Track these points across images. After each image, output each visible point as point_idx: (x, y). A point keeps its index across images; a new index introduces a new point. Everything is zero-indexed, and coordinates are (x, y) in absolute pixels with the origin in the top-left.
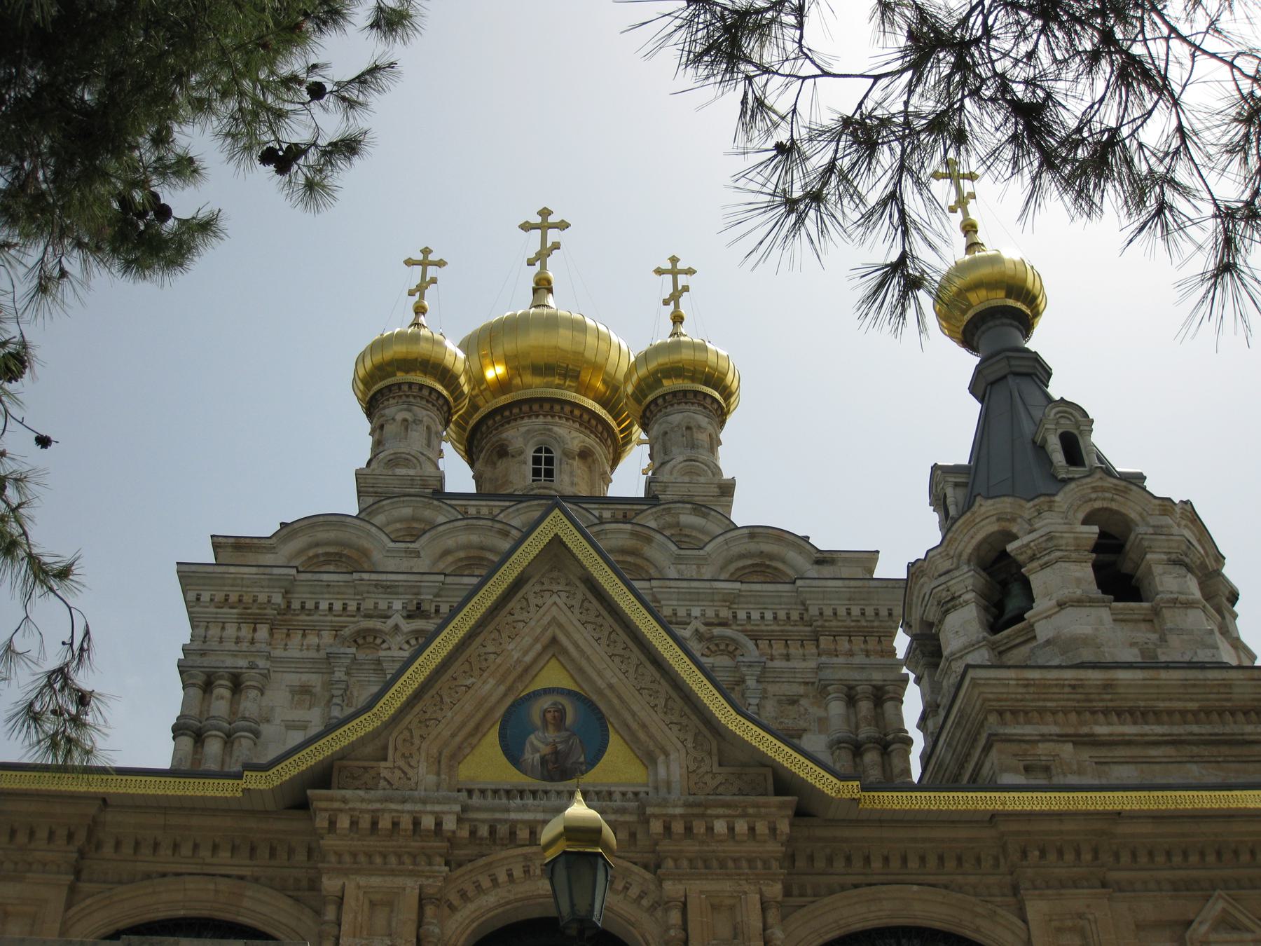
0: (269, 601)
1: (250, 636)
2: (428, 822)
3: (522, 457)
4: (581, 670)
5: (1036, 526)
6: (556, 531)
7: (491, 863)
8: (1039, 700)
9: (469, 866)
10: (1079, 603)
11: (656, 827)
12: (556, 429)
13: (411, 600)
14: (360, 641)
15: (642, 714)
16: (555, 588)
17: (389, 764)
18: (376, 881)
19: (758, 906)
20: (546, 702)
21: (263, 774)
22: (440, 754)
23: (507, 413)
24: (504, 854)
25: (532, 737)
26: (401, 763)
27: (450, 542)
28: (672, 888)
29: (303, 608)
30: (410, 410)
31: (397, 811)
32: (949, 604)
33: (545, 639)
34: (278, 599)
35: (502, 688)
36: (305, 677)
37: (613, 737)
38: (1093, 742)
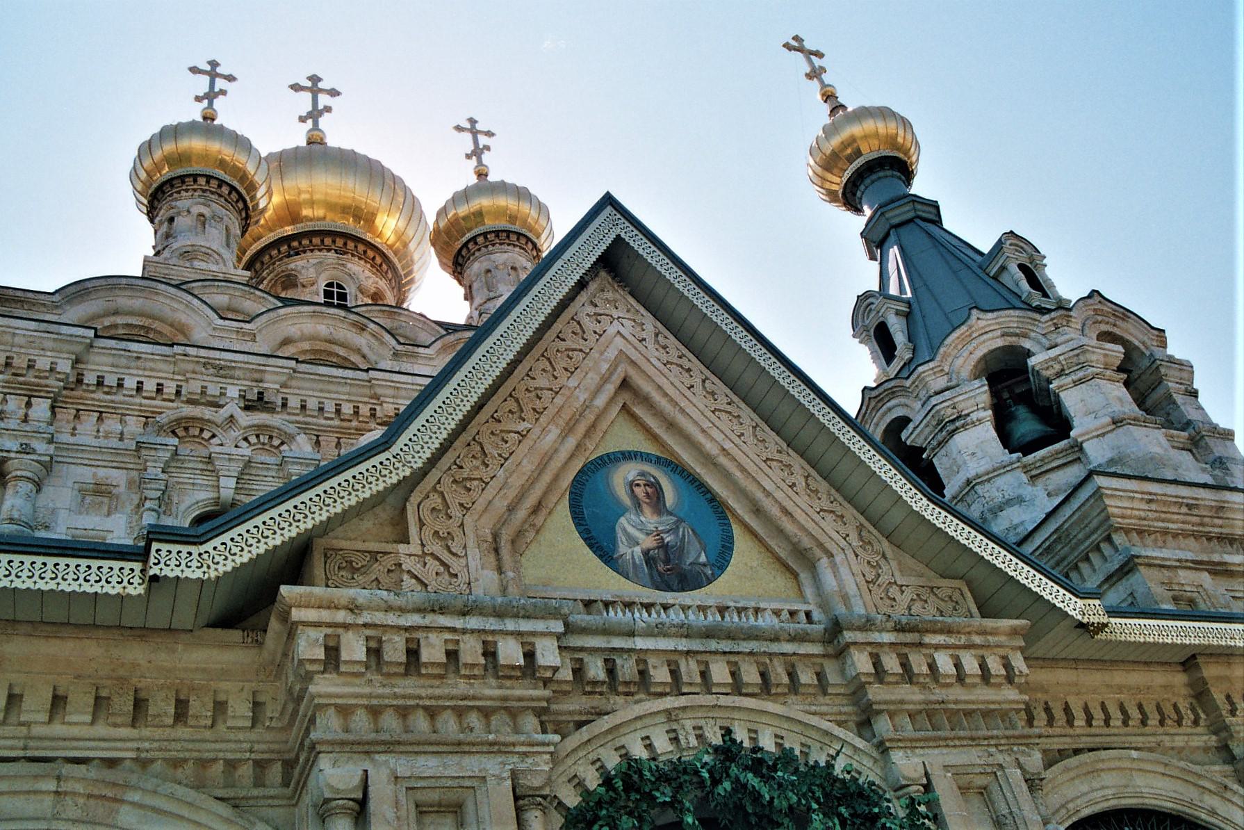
0: (52, 370)
1: (22, 412)
2: (510, 652)
3: (315, 287)
4: (671, 425)
5: (1059, 340)
6: (618, 231)
7: (616, 727)
8: (1163, 521)
9: (584, 734)
10: (1135, 421)
11: (861, 663)
12: (349, 265)
13: (251, 388)
14: (181, 432)
15: (779, 495)
16: (615, 314)
17: (414, 548)
18: (428, 765)
19: (1025, 787)
21: (195, 550)
22: (496, 536)
23: (295, 244)
24: (638, 710)
25: (622, 520)
26: (435, 547)
27: (293, 330)
29: (100, 383)
30: (209, 206)
31: (453, 630)
33: (617, 379)
34: (65, 366)
35: (571, 442)
36: (102, 472)
37: (736, 530)
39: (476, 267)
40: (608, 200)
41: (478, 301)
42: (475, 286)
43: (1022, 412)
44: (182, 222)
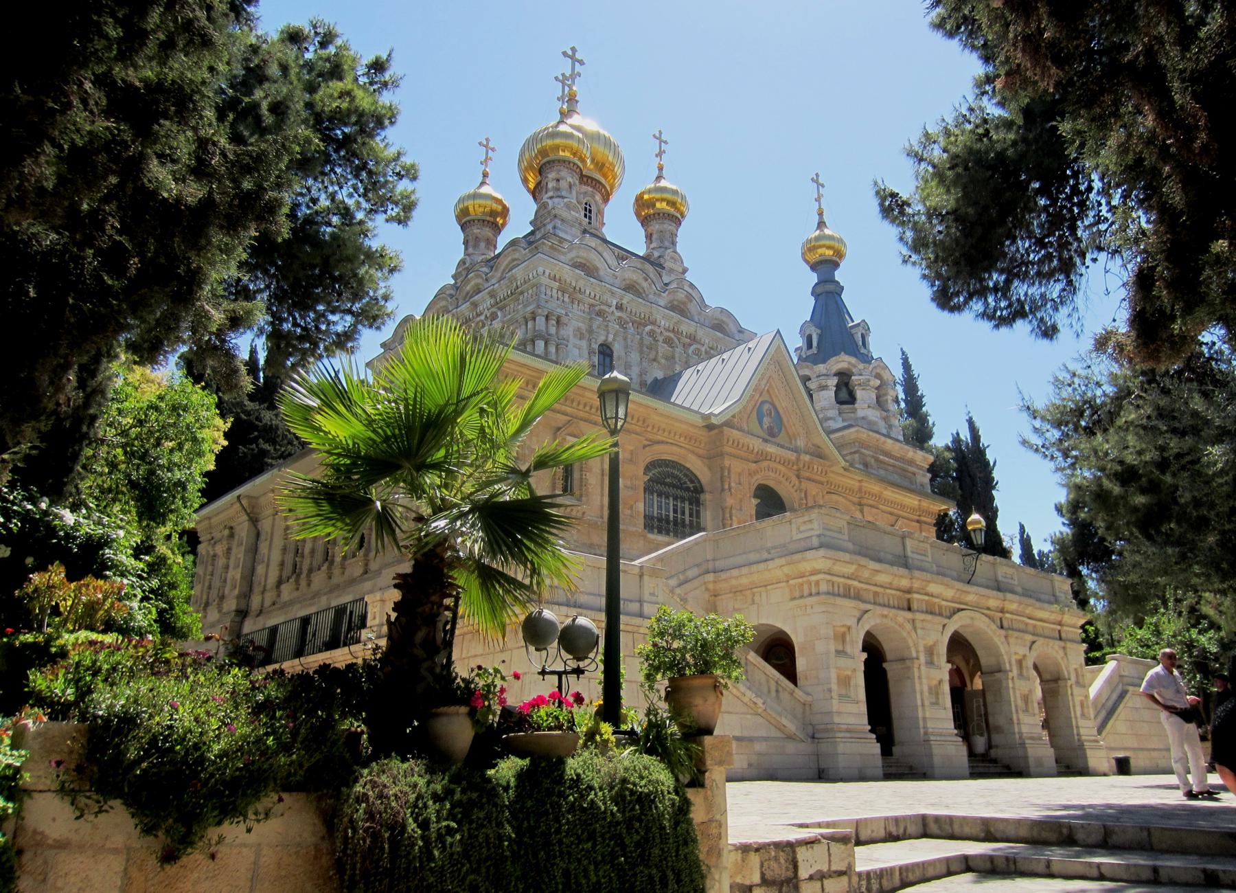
20: (766, 406)
28: (803, 486)
32: (823, 388)
38: (877, 460)
39: (655, 227)
40: (778, 331)
41: (654, 245)
42: (654, 237)
43: (844, 390)
44: (563, 184)
